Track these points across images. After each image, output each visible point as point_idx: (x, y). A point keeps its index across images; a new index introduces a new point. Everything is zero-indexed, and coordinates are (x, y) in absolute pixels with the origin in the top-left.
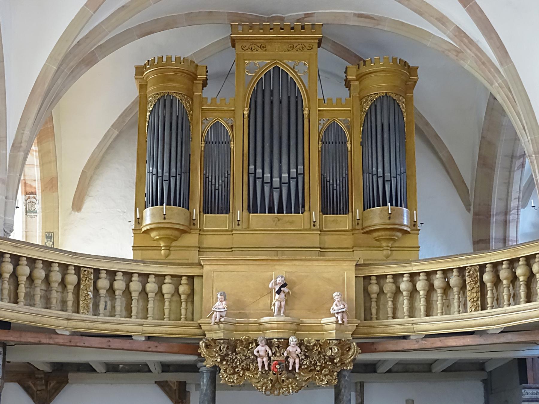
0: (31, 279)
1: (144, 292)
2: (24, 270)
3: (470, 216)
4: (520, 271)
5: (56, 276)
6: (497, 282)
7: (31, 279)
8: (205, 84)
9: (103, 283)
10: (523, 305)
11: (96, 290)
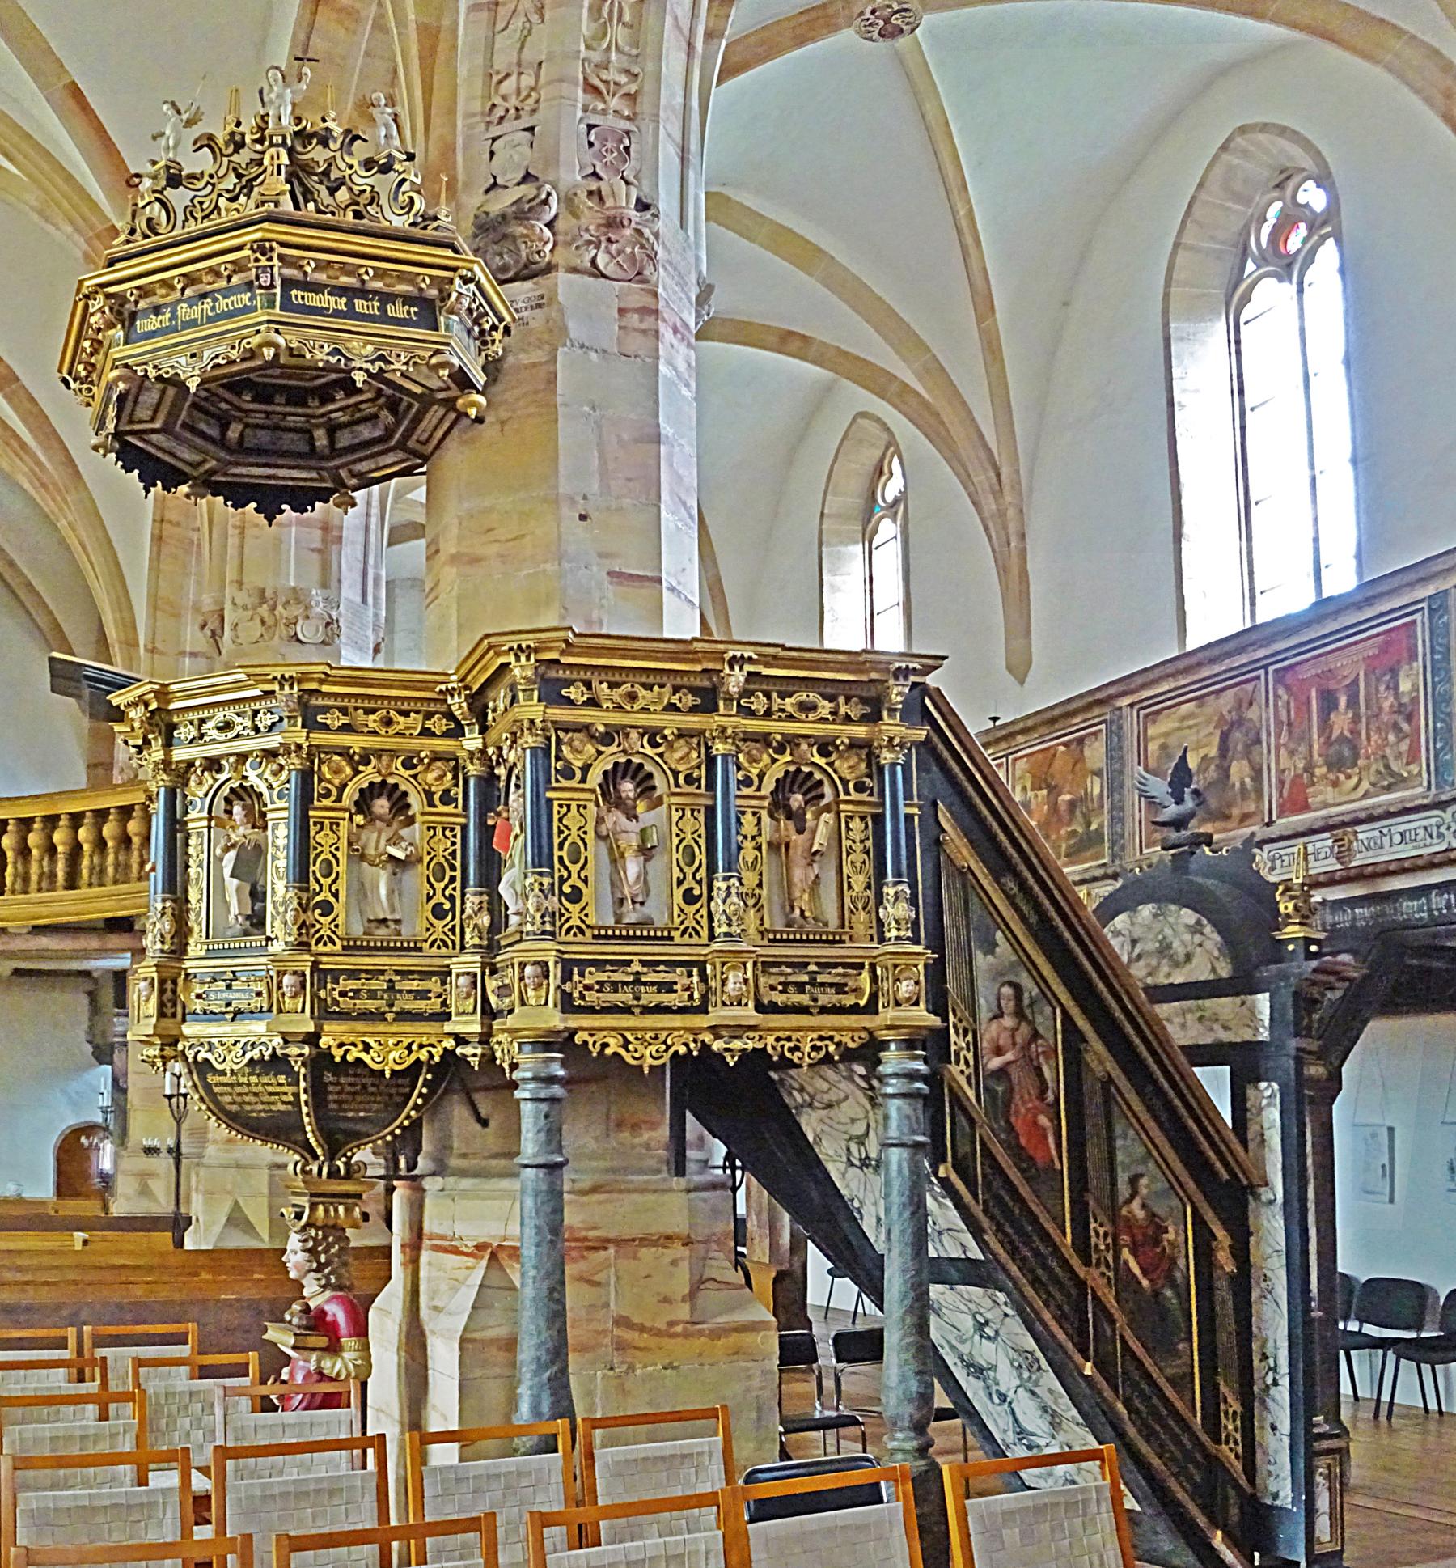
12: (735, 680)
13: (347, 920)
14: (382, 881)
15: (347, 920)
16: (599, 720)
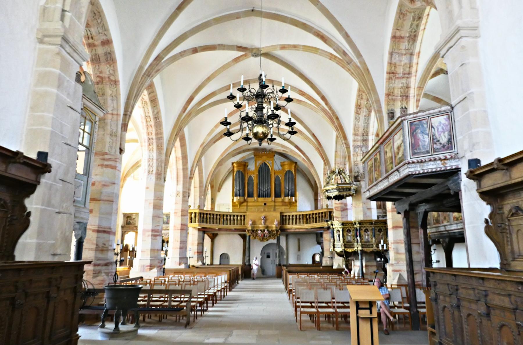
0: (210, 218)
1: (234, 219)
2: (209, 216)
3: (314, 193)
4: (314, 216)
5: (215, 217)
6: (310, 218)
7: (210, 218)
8: (248, 166)
9: (225, 217)
10: (315, 224)
11: (224, 219)
12: (374, 223)
13: (346, 240)
14: (349, 237)
15: (346, 240)
16: (364, 226)
